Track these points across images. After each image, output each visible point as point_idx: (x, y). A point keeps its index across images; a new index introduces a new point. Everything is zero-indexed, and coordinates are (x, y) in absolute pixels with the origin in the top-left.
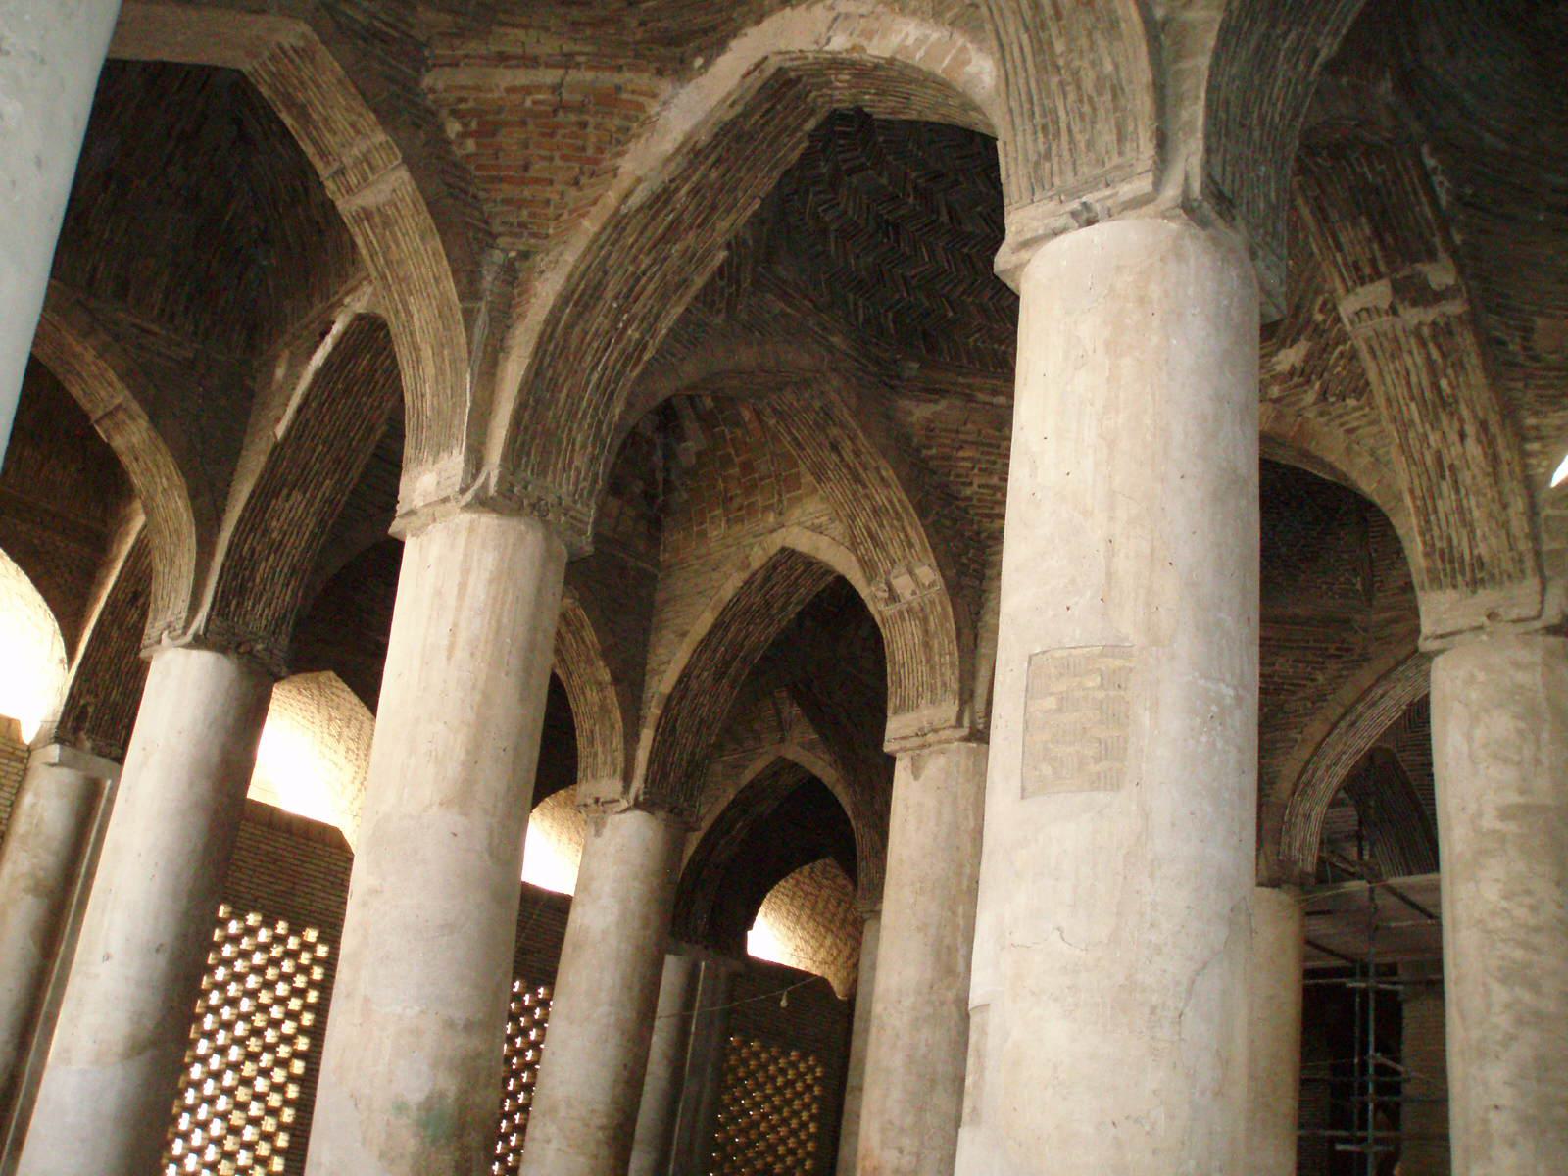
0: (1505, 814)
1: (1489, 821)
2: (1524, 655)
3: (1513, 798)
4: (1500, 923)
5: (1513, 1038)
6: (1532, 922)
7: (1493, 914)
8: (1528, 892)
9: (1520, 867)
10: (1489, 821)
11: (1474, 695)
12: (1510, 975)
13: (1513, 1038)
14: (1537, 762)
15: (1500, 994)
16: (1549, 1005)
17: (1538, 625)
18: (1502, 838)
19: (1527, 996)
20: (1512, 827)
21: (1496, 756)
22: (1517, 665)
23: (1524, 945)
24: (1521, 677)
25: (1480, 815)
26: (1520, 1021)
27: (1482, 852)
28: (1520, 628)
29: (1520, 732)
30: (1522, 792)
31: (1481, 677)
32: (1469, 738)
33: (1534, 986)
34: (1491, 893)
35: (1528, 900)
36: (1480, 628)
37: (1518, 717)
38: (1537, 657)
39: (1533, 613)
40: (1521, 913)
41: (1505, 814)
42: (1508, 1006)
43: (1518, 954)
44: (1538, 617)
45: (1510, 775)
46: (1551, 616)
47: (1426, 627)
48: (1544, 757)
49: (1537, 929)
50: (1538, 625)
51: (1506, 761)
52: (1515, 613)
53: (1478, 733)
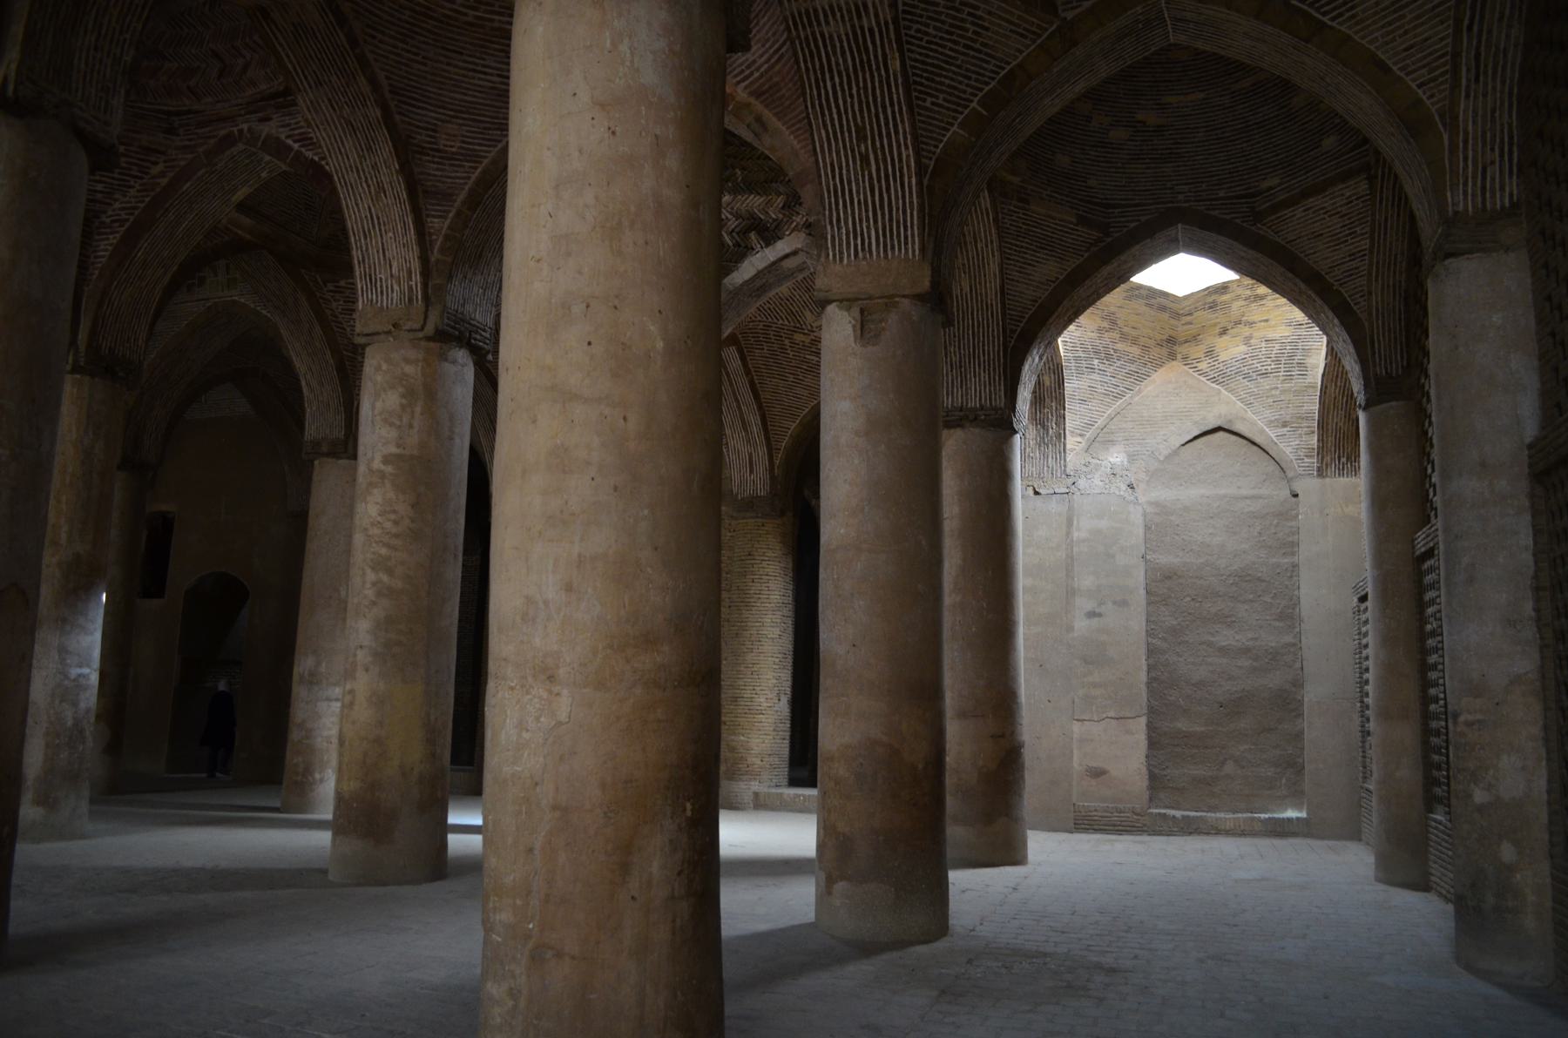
0: (387, 460)
1: (377, 464)
2: (412, 354)
3: (393, 450)
4: (376, 531)
5: (374, 603)
6: (394, 530)
7: (373, 524)
8: (394, 512)
9: (391, 495)
10: (377, 464)
11: (379, 378)
12: (379, 564)
13: (374, 603)
14: (411, 426)
15: (371, 576)
16: (398, 584)
17: (421, 335)
18: (383, 475)
19: (385, 578)
20: (389, 469)
21: (385, 420)
22: (407, 361)
23: (388, 546)
24: (409, 369)
25: (373, 459)
26: (379, 594)
27: (371, 484)
28: (411, 336)
29: (403, 407)
30: (398, 446)
31: (384, 367)
32: (373, 408)
33: (390, 572)
34: (373, 510)
35: (393, 517)
36: (389, 333)
37: (403, 396)
38: (420, 356)
39: (417, 326)
40: (388, 525)
41: (387, 460)
42: (374, 584)
43: (384, 551)
44: (422, 329)
45: (392, 434)
46: (430, 329)
47: (358, 330)
48: (416, 424)
49: (397, 536)
50: (421, 335)
51: (391, 425)
52: (409, 325)
53: (379, 405)
